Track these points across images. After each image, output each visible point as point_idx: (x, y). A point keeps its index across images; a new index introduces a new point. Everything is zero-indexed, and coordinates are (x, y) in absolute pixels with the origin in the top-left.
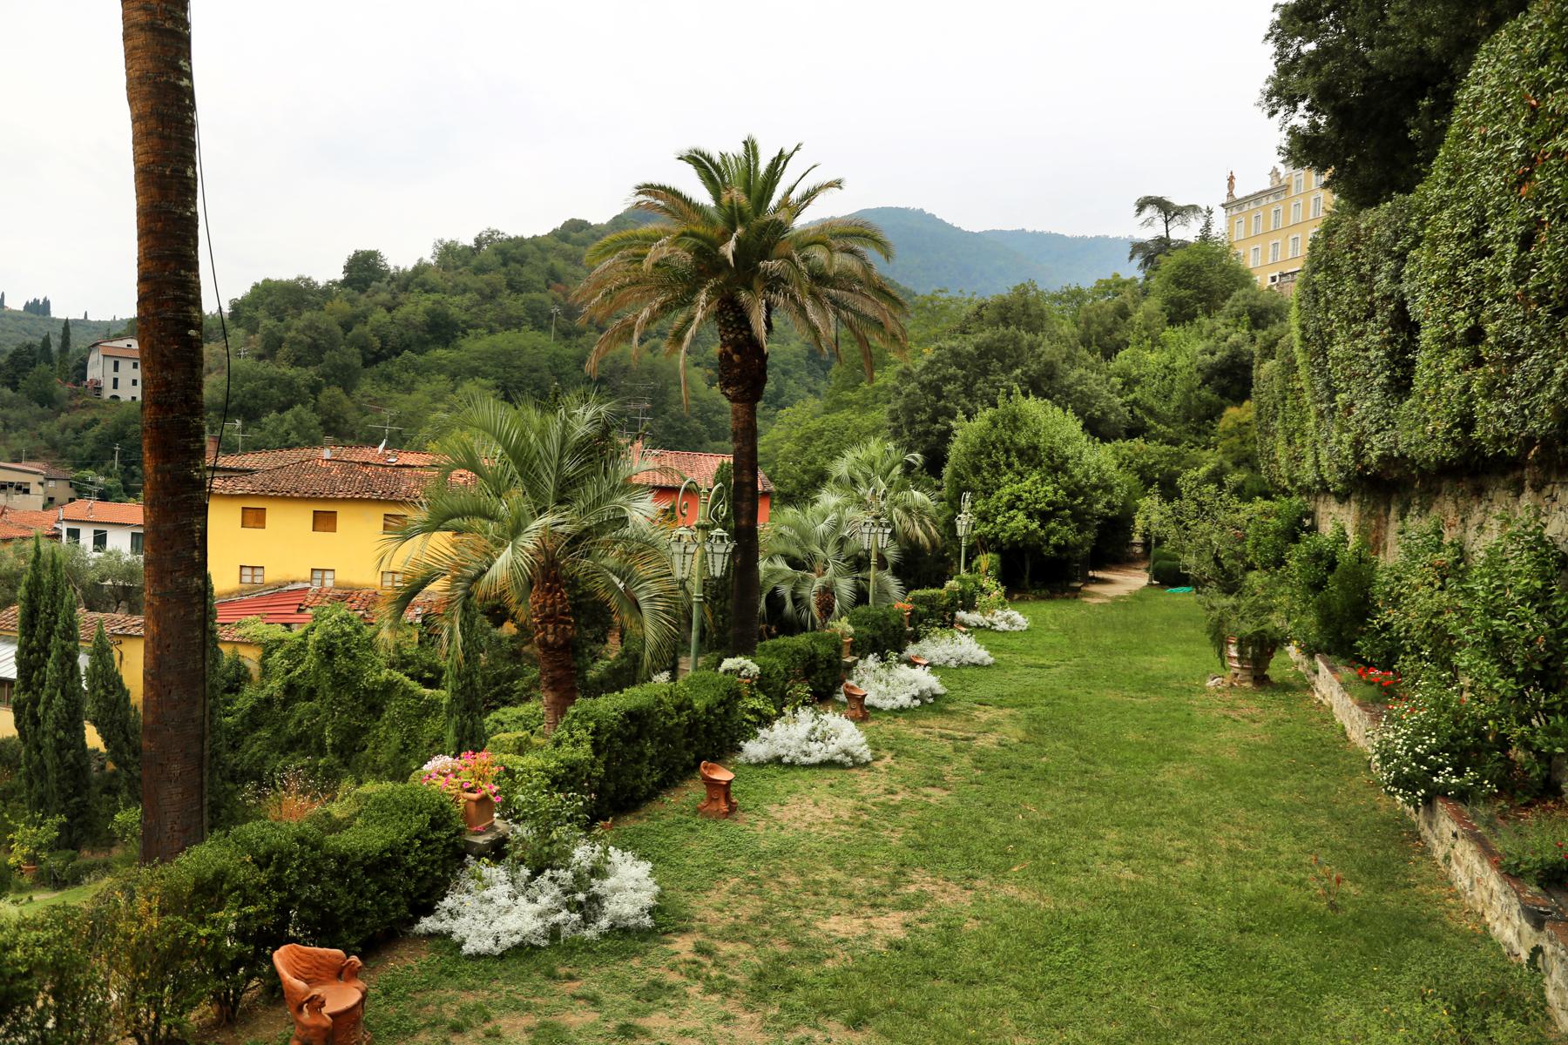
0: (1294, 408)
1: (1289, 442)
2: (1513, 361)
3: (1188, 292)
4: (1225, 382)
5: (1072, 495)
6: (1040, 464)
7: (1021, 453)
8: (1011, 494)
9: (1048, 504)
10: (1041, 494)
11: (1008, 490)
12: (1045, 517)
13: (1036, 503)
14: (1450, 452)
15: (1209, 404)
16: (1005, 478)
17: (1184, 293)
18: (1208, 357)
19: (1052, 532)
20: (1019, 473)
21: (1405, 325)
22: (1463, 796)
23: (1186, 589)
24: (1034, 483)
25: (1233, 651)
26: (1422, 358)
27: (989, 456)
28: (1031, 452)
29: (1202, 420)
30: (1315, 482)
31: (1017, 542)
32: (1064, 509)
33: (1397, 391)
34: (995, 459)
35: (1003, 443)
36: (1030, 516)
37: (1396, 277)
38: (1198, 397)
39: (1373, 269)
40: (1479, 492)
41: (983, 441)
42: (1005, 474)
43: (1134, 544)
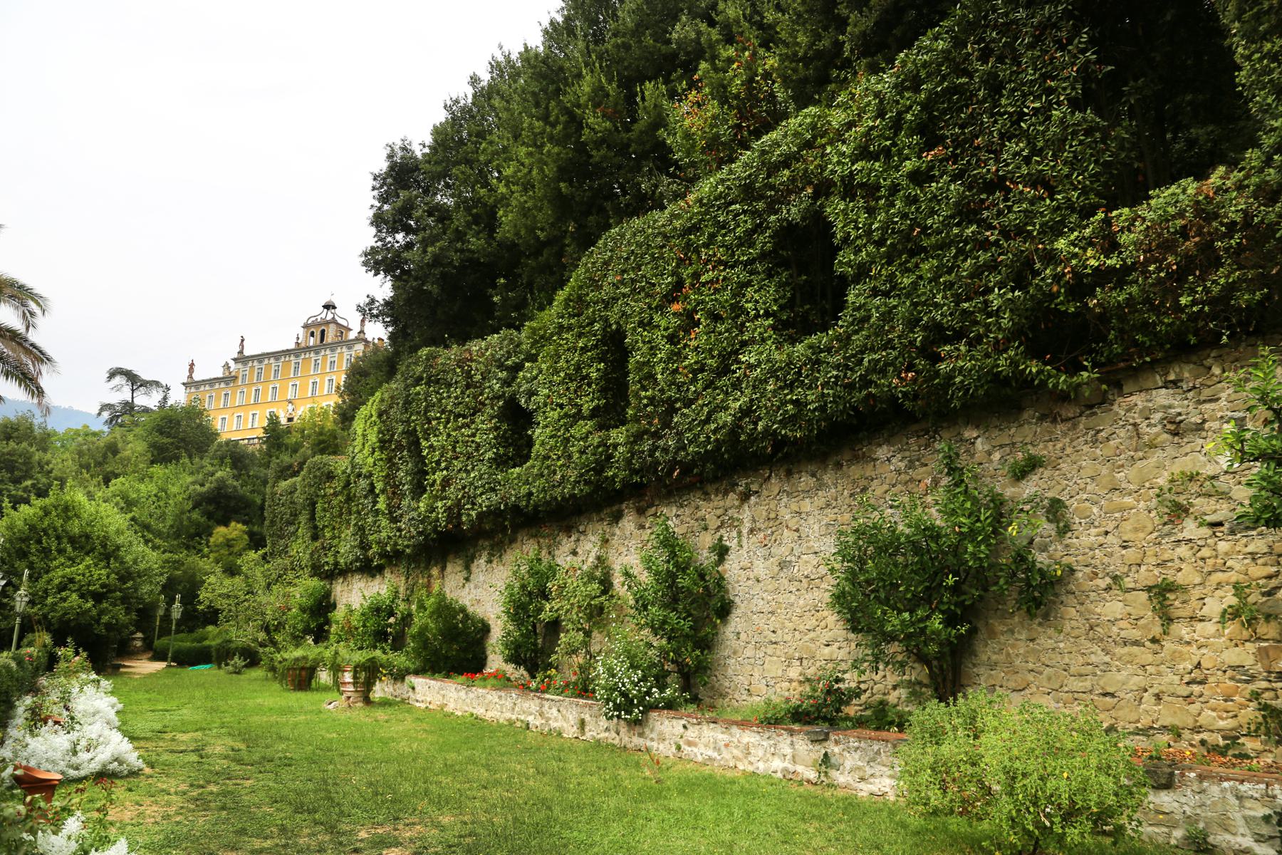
0: (324, 510)
1: (315, 538)
3: (169, 440)
4: (211, 508)
5: (123, 579)
6: (93, 550)
7: (72, 540)
8: (63, 577)
9: (103, 586)
10: (96, 577)
11: (60, 573)
12: (98, 597)
13: (89, 585)
15: (198, 524)
16: (55, 563)
17: (166, 440)
18: (198, 487)
19: (101, 613)
20: (70, 559)
22: (670, 705)
23: (208, 666)
24: (88, 567)
25: (348, 677)
26: (538, 433)
27: (39, 542)
28: (83, 539)
29: (191, 537)
30: (357, 559)
31: (70, 620)
32: (114, 591)
33: (498, 466)
34: (45, 545)
35: (55, 529)
36: (82, 596)
37: (507, 383)
38: (189, 518)
39: (484, 378)
41: (32, 528)
42: (55, 559)
43: (134, 639)
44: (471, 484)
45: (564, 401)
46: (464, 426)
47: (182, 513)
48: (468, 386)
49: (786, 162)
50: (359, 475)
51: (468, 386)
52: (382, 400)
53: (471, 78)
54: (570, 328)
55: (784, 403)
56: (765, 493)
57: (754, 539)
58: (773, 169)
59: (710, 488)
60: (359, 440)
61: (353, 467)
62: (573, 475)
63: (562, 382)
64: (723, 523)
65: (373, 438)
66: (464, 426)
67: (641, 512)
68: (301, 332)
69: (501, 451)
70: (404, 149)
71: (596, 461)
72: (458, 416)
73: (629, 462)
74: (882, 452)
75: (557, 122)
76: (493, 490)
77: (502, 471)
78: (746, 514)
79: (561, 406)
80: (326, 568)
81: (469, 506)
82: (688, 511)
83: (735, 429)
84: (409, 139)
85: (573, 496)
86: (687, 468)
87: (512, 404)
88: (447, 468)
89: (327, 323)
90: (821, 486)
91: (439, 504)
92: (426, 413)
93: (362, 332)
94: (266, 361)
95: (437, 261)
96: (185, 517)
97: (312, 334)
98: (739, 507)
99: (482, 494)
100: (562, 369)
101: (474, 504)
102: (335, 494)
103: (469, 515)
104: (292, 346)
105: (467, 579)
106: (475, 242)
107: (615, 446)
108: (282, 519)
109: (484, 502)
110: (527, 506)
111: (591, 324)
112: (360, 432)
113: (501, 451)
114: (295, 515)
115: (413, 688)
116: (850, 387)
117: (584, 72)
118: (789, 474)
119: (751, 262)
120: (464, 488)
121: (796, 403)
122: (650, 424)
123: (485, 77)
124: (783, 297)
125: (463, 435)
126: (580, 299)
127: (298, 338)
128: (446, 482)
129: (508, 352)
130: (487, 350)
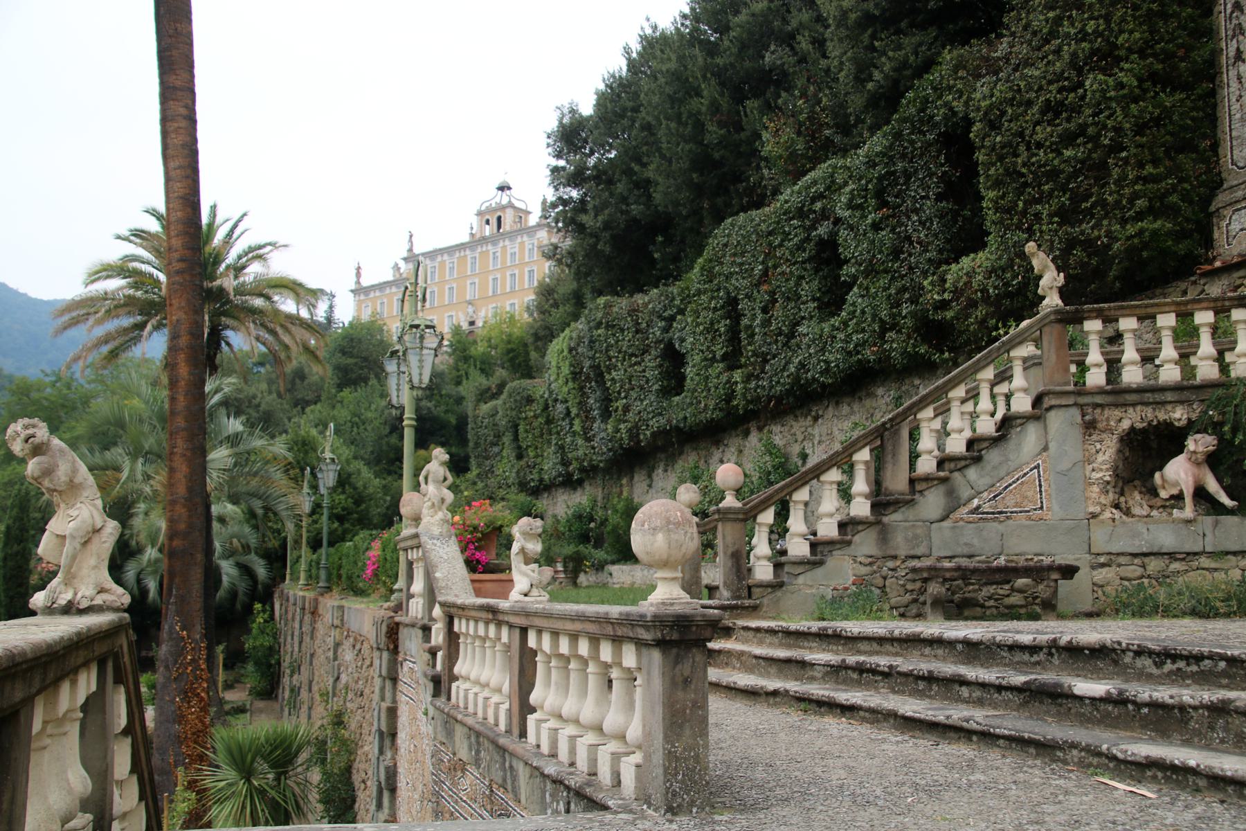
0: (526, 431)
1: (520, 457)
2: (766, 361)
5: (358, 502)
9: (344, 509)
10: (337, 501)
14: (717, 415)
17: (350, 361)
21: (673, 359)
26: (689, 371)
30: (560, 475)
32: (352, 514)
37: (666, 330)
38: (388, 444)
39: (648, 326)
40: (717, 443)
44: (645, 410)
45: (704, 348)
46: (635, 364)
47: (381, 438)
48: (637, 332)
49: (821, 196)
50: (556, 400)
51: (637, 332)
52: (571, 338)
53: (625, 48)
54: (705, 291)
55: (819, 361)
56: (826, 417)
57: (821, 448)
59: (798, 413)
60: (554, 370)
61: (551, 393)
62: (712, 404)
63: (701, 333)
64: (805, 437)
65: (566, 370)
66: (635, 364)
67: (760, 429)
68: (475, 221)
69: (665, 383)
71: (725, 394)
72: (633, 355)
73: (744, 395)
74: (880, 391)
75: (687, 124)
76: (660, 414)
77: (667, 399)
78: (816, 431)
79: (702, 351)
80: (532, 484)
81: (644, 427)
82: (786, 428)
83: (796, 378)
84: (575, 101)
85: (712, 419)
86: (779, 399)
87: (670, 345)
88: (626, 397)
89: (503, 208)
90: (853, 413)
91: (622, 426)
92: (607, 351)
94: (439, 259)
95: (607, 226)
96: (384, 442)
97: (488, 222)
98: (813, 426)
99: (653, 417)
100: (701, 324)
101: (648, 426)
102: (536, 417)
103: (645, 434)
104: (466, 238)
105: (650, 486)
106: (636, 209)
107: (736, 383)
108: (486, 440)
109: (656, 424)
110: (685, 427)
111: (718, 290)
112: (554, 363)
113: (665, 383)
114: (498, 436)
115: (611, 574)
116: (849, 353)
117: (703, 86)
118: (837, 403)
119: (803, 262)
120: (640, 412)
121: (825, 361)
122: (755, 369)
123: (636, 47)
124: (826, 285)
125: (636, 371)
126: (710, 271)
127: (472, 228)
128: (626, 409)
129: (665, 306)
130: (649, 302)
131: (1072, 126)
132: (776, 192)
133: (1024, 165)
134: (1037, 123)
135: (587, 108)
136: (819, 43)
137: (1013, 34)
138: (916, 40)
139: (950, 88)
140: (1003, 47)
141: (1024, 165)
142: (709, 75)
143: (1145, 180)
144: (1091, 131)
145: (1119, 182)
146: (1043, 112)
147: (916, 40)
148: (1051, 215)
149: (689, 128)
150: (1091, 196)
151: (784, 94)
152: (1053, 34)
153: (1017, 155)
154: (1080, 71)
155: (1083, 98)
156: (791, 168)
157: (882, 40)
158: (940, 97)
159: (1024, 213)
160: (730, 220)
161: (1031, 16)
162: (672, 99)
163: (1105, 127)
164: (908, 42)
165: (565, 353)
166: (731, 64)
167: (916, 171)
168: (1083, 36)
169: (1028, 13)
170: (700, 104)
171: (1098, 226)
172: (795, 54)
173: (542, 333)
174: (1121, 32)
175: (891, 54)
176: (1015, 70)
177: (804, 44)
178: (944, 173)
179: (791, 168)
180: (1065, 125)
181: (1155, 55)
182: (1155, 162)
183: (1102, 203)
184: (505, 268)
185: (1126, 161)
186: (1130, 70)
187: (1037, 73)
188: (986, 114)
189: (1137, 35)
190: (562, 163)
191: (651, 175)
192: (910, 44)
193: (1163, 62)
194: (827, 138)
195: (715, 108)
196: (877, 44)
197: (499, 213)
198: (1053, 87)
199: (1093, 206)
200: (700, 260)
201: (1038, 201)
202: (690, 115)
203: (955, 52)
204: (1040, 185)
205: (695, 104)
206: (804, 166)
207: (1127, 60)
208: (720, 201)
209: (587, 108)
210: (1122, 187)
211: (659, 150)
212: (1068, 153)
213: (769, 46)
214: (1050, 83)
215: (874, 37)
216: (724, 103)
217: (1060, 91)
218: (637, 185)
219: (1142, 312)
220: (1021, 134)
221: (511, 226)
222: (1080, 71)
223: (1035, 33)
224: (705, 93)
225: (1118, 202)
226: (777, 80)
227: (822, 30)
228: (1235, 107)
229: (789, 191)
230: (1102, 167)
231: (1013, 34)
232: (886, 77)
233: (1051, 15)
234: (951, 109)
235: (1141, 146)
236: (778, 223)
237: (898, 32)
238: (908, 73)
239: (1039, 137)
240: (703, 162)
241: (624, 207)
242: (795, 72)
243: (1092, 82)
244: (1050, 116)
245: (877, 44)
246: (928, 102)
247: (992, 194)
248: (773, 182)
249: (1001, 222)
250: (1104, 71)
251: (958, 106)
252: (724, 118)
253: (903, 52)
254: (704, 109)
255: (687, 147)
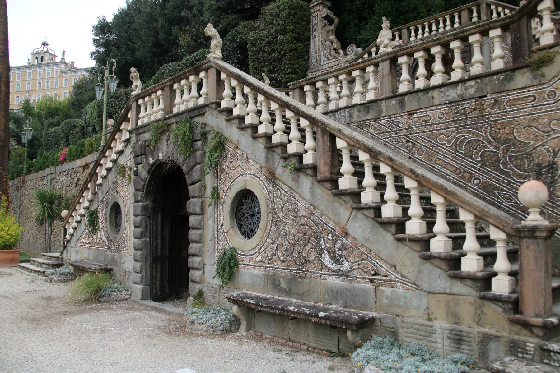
0: (72, 138)
49: (199, 60)
50: (88, 126)
58: (196, 61)
70: (104, 20)
89: (45, 53)
92: (114, 107)
93: (63, 58)
102: (77, 133)
108: (51, 143)
112: (90, 112)
131: (274, 48)
132: (182, 58)
133: (261, 57)
134: (265, 46)
135: (110, 19)
136: (200, 11)
137: (261, 21)
138: (233, 17)
139: (242, 33)
140: (257, 24)
141: (261, 57)
142: (162, 16)
143: (291, 64)
144: (279, 50)
145: (284, 64)
146: (267, 43)
147: (233, 17)
148: (267, 71)
149: (152, 33)
150: (278, 67)
151: (188, 26)
152: (271, 23)
153: (259, 54)
154: (277, 34)
155: (277, 41)
156: (188, 50)
157: (222, 15)
158: (239, 35)
159: (260, 70)
160: (166, 65)
161: (266, 17)
162: (147, 22)
163: (282, 49)
164: (231, 17)
165: (96, 107)
166: (170, 14)
167: (230, 55)
168: (278, 25)
169: (265, 16)
170: (158, 25)
171: (279, 75)
172: (191, 13)
173: (75, 103)
174: (288, 25)
175: (225, 20)
176: (261, 31)
177: (195, 10)
178: (238, 57)
179: (188, 50)
180: (273, 47)
181: (295, 33)
182: (294, 60)
183: (280, 69)
184: (53, 78)
185: (287, 59)
186: (289, 36)
187: (266, 32)
188: (252, 41)
189: (291, 27)
190: (98, 38)
191: (137, 46)
192: (231, 18)
193: (297, 35)
194: (201, 42)
195: (163, 27)
196: (221, 16)
197: (42, 55)
198: (270, 37)
199: (278, 70)
200: (154, 77)
201: (264, 67)
202: (154, 28)
203: (244, 23)
204: (265, 63)
205: (155, 25)
206: (192, 50)
207: (289, 33)
208: (161, 58)
209: (110, 19)
210: (285, 65)
211: (141, 38)
212: (273, 55)
213: (183, 9)
214: (270, 36)
215: (220, 14)
216: (166, 26)
217: (272, 38)
218: (129, 49)
219: (286, 91)
220: (261, 48)
221: (48, 61)
222: (277, 34)
223: (266, 22)
224: (160, 21)
225: (284, 69)
226: (186, 21)
227: (201, 7)
228: (313, 49)
229: (188, 57)
230: (281, 60)
231: (261, 21)
232: (223, 27)
233: (271, 18)
234: (242, 39)
235: (291, 55)
236: (184, 67)
237: (228, 14)
238: (230, 26)
239: (266, 50)
240: (157, 44)
241: (124, 57)
242: (192, 19)
243: (280, 37)
244: (269, 44)
245: (221, 16)
246: (235, 35)
247: (252, 64)
248: (181, 54)
249: (254, 71)
250: (283, 35)
251: (244, 38)
252: (166, 31)
253: (229, 20)
254: (159, 27)
255: (152, 39)
